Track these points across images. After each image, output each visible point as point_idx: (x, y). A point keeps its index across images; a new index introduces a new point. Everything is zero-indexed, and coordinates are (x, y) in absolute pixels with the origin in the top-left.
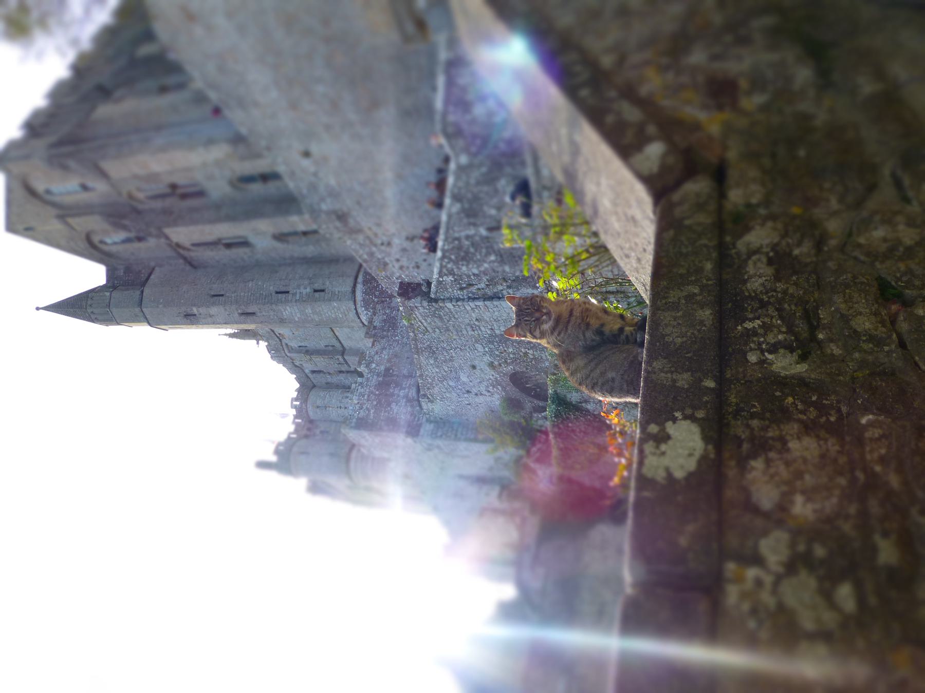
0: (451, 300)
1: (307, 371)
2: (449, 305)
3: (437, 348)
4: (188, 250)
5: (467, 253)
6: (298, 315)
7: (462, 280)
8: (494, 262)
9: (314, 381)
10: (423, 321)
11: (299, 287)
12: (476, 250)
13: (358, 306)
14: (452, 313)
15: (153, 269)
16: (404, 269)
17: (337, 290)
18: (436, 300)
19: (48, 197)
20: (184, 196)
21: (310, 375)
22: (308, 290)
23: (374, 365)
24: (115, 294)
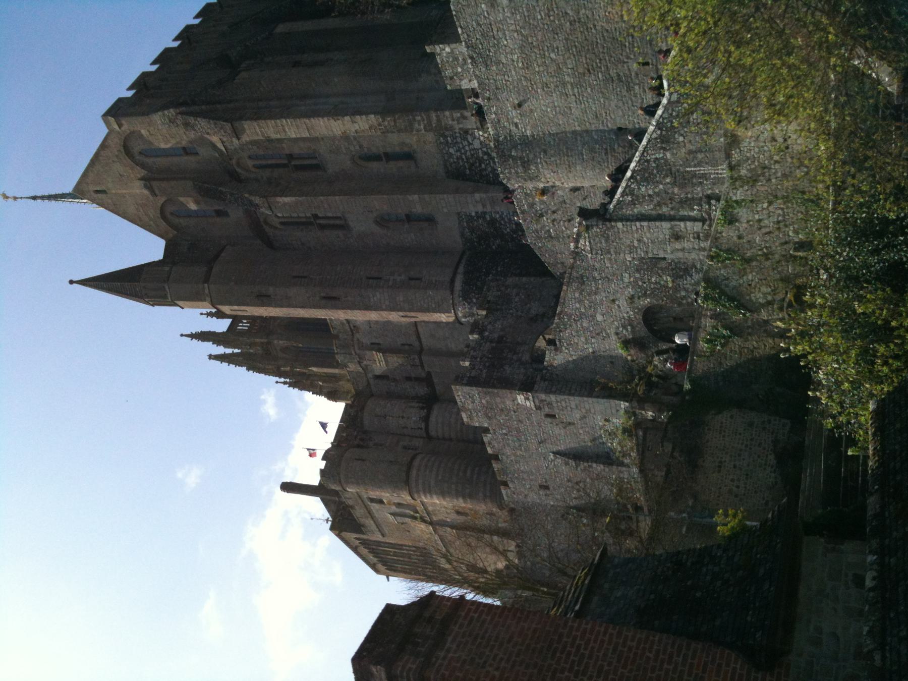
0: (621, 220)
2: (620, 225)
3: (588, 278)
4: (276, 228)
5: (651, 174)
7: (637, 200)
8: (668, 183)
12: (658, 173)
16: (555, 223)
18: (610, 220)
19: (138, 157)
21: (372, 381)
22: (403, 277)
23: (487, 333)
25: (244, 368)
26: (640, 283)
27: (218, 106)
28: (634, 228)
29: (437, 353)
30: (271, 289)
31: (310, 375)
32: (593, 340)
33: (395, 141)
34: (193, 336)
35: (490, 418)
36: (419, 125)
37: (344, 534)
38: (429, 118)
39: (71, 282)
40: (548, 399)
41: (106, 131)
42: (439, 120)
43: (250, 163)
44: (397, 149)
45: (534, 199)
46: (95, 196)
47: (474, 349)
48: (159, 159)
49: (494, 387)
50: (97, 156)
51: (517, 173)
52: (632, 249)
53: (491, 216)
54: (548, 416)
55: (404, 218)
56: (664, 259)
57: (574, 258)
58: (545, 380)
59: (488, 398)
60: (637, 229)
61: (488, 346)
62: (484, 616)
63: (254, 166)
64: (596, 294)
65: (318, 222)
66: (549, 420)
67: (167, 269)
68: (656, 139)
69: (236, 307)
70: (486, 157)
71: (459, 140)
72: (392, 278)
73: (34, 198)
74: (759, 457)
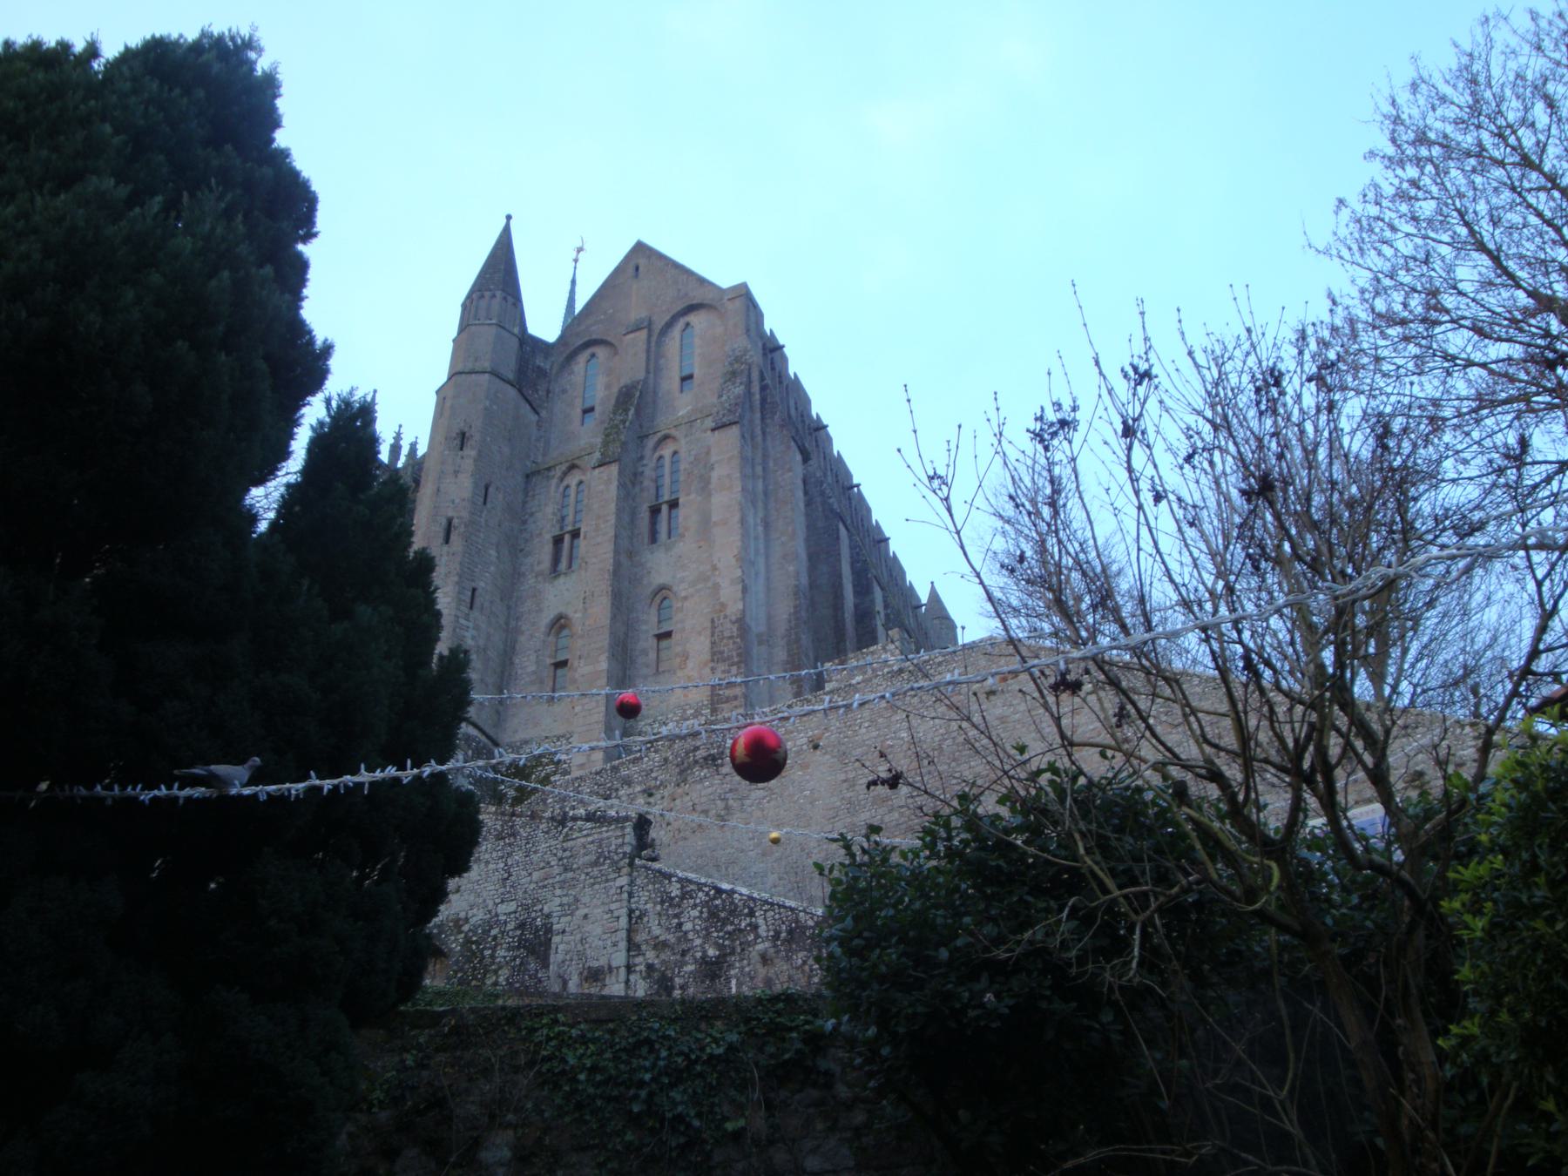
2: (624, 881)
3: (510, 845)
4: (562, 480)
5: (725, 922)
8: (704, 952)
10: (590, 839)
11: (477, 628)
14: (607, 881)
15: (537, 413)
18: (631, 864)
19: (681, 322)
20: (655, 511)
24: (514, 343)
26: (493, 932)
27: (758, 415)
28: (613, 906)
30: (473, 453)
39: (509, 217)
42: (728, 700)
45: (640, 783)
51: (697, 748)
55: (561, 658)
56: (546, 965)
57: (552, 819)
60: (612, 911)
63: (661, 457)
67: (516, 330)
68: (797, 921)
72: (471, 625)
73: (573, 282)
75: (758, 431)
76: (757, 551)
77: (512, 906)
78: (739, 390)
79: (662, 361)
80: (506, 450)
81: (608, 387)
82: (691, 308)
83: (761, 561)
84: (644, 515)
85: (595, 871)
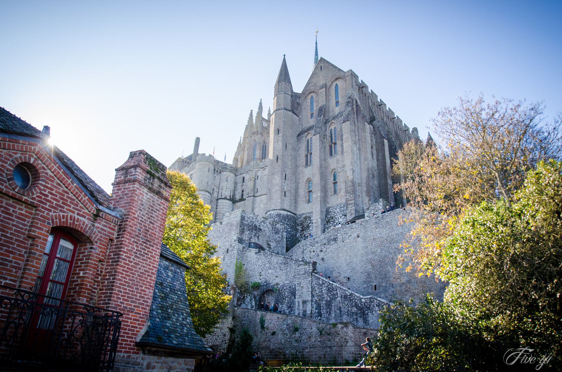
1: (244, 175)
2: (310, 279)
4: (306, 137)
6: (275, 182)
9: (238, 177)
11: (287, 185)
13: (278, 211)
17: (285, 202)
18: (312, 275)
19: (335, 83)
20: (331, 147)
21: (242, 176)
22: (286, 189)
23: (263, 224)
24: (290, 96)
25: (247, 124)
26: (285, 288)
27: (356, 115)
28: (308, 285)
29: (253, 203)
31: (244, 151)
32: (260, 269)
33: (341, 186)
34: (261, 103)
35: (227, 225)
36: (349, 196)
37: (177, 163)
38: (351, 200)
39: (284, 55)
40: (235, 249)
41: (345, 71)
43: (333, 128)
44: (339, 187)
46: (320, 66)
47: (256, 218)
48: (334, 91)
49: (241, 226)
50: (336, 67)
51: (331, 236)
52: (299, 284)
53: (311, 226)
54: (228, 249)
55: (310, 189)
56: (295, 298)
58: (243, 249)
59: (235, 224)
60: (308, 286)
61: (258, 224)
62: (161, 211)
64: (280, 269)
65: (309, 155)
66: (226, 250)
67: (290, 93)
69: (274, 120)
70: (335, 224)
71: (342, 213)
74: (211, 339)
75: (356, 121)
76: (357, 158)
77: (288, 282)
78: (349, 109)
79: (330, 97)
80: (290, 132)
81: (317, 106)
82: (337, 79)
83: (358, 161)
84: (328, 148)
85: (304, 276)
